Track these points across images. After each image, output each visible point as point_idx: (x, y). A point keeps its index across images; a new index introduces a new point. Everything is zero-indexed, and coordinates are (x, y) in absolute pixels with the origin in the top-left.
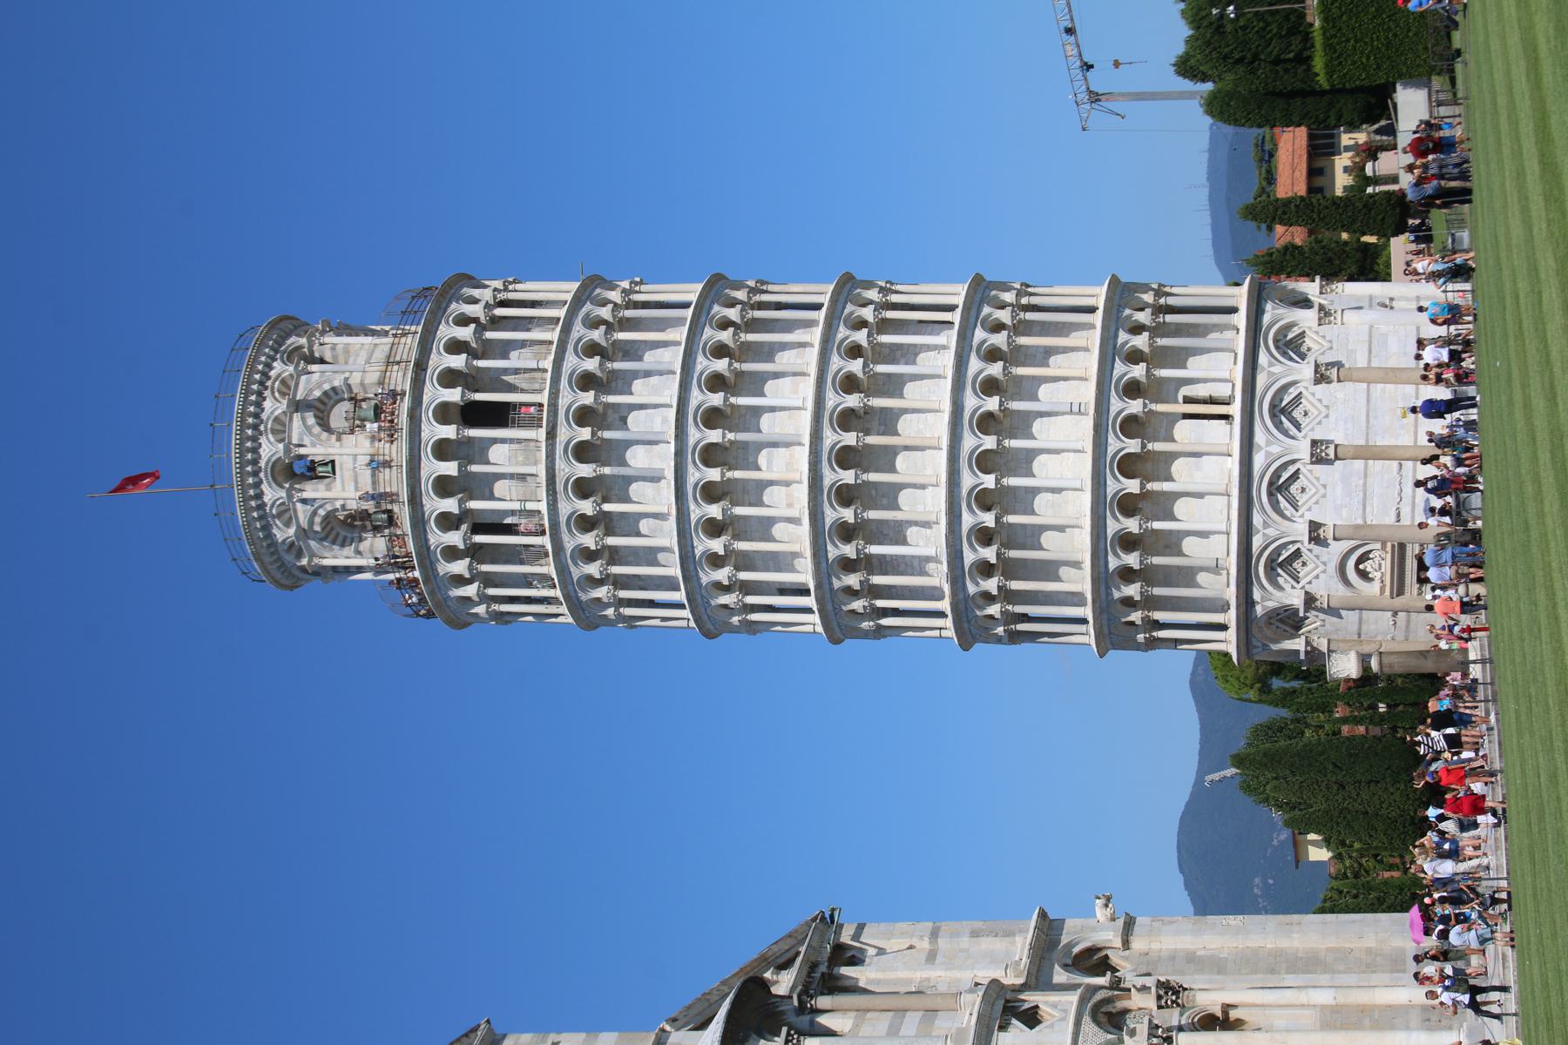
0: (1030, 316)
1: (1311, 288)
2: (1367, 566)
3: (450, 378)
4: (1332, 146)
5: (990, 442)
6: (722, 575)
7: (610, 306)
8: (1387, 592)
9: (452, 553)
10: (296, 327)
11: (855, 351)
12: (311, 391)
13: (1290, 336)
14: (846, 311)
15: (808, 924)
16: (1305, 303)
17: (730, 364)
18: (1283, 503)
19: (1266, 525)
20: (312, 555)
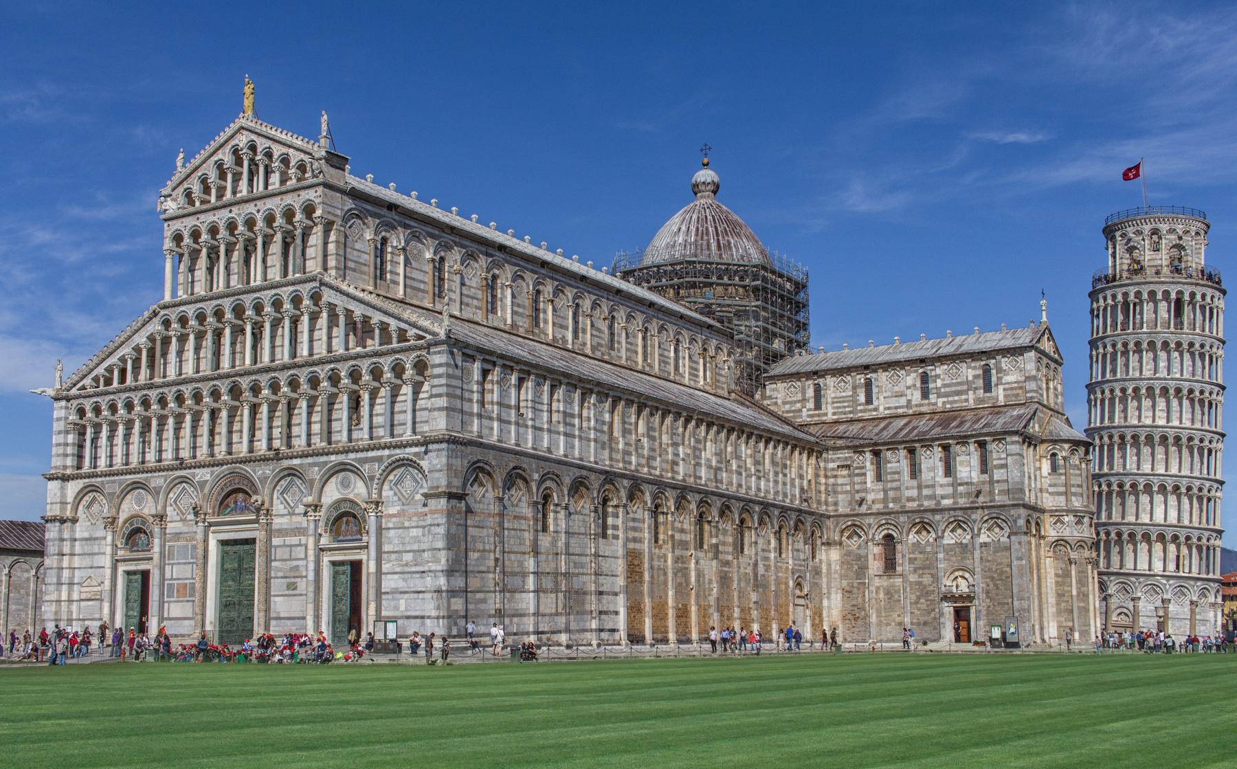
2: (1123, 616)
3: (1193, 295)
6: (1118, 393)
9: (1125, 295)
16: (1216, 597)
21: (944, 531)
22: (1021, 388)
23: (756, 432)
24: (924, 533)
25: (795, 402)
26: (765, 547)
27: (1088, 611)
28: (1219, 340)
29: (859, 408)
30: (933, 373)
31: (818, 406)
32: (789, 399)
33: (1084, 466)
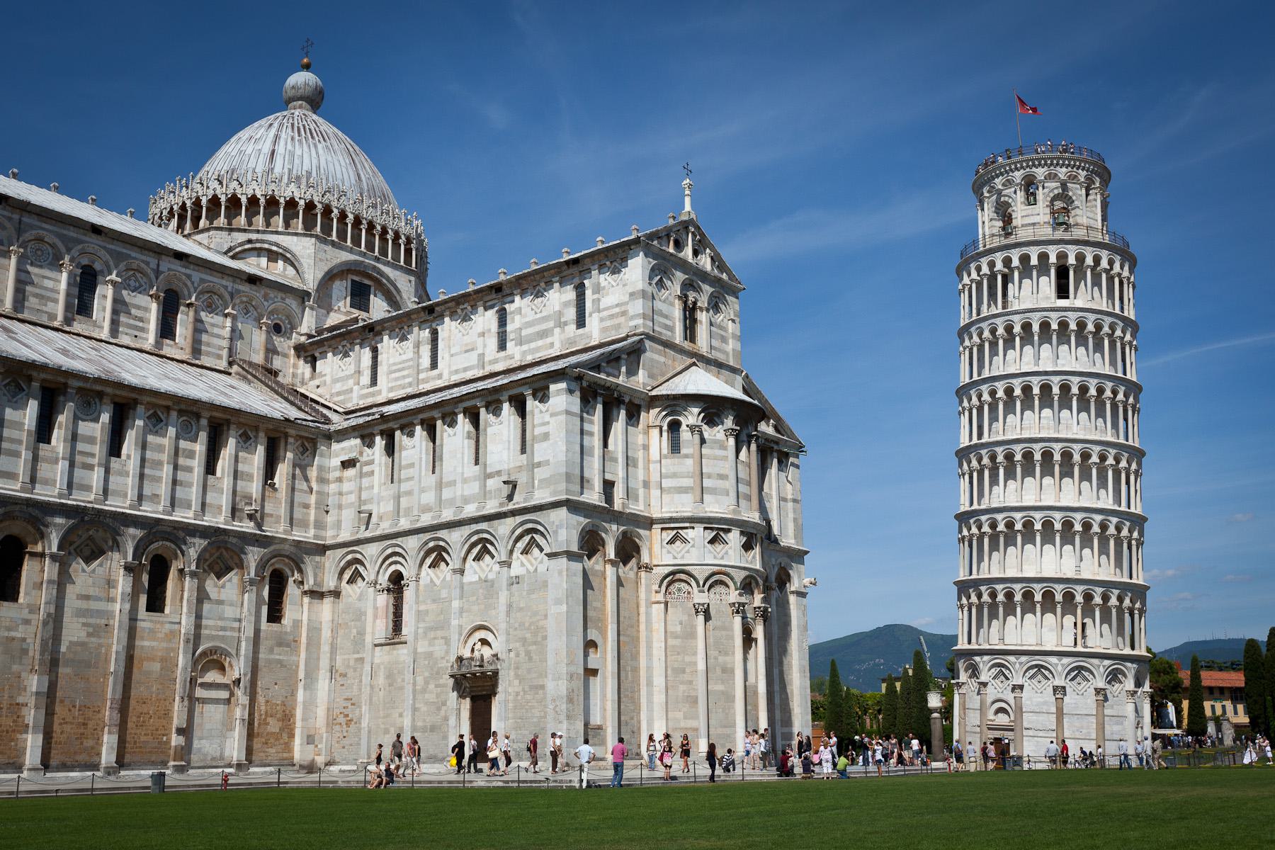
0: (1125, 545)
1: (1147, 687)
3: (1080, 258)
4: (1237, 699)
5: (1058, 526)
7: (1122, 335)
8: (989, 723)
9: (992, 264)
10: (1105, 181)
11: (1103, 458)
12: (1072, 191)
13: (1120, 676)
14: (1124, 453)
15: (798, 440)
16: (1139, 684)
17: (1093, 396)
18: (1032, 672)
19: (1021, 663)
20: (989, 198)
21: (465, 559)
22: (624, 313)
23: (75, 383)
24: (443, 564)
25: (348, 377)
26: (91, 592)
27: (730, 698)
28: (1125, 320)
29: (422, 376)
30: (512, 309)
31: (374, 381)
32: (341, 374)
33: (732, 441)
